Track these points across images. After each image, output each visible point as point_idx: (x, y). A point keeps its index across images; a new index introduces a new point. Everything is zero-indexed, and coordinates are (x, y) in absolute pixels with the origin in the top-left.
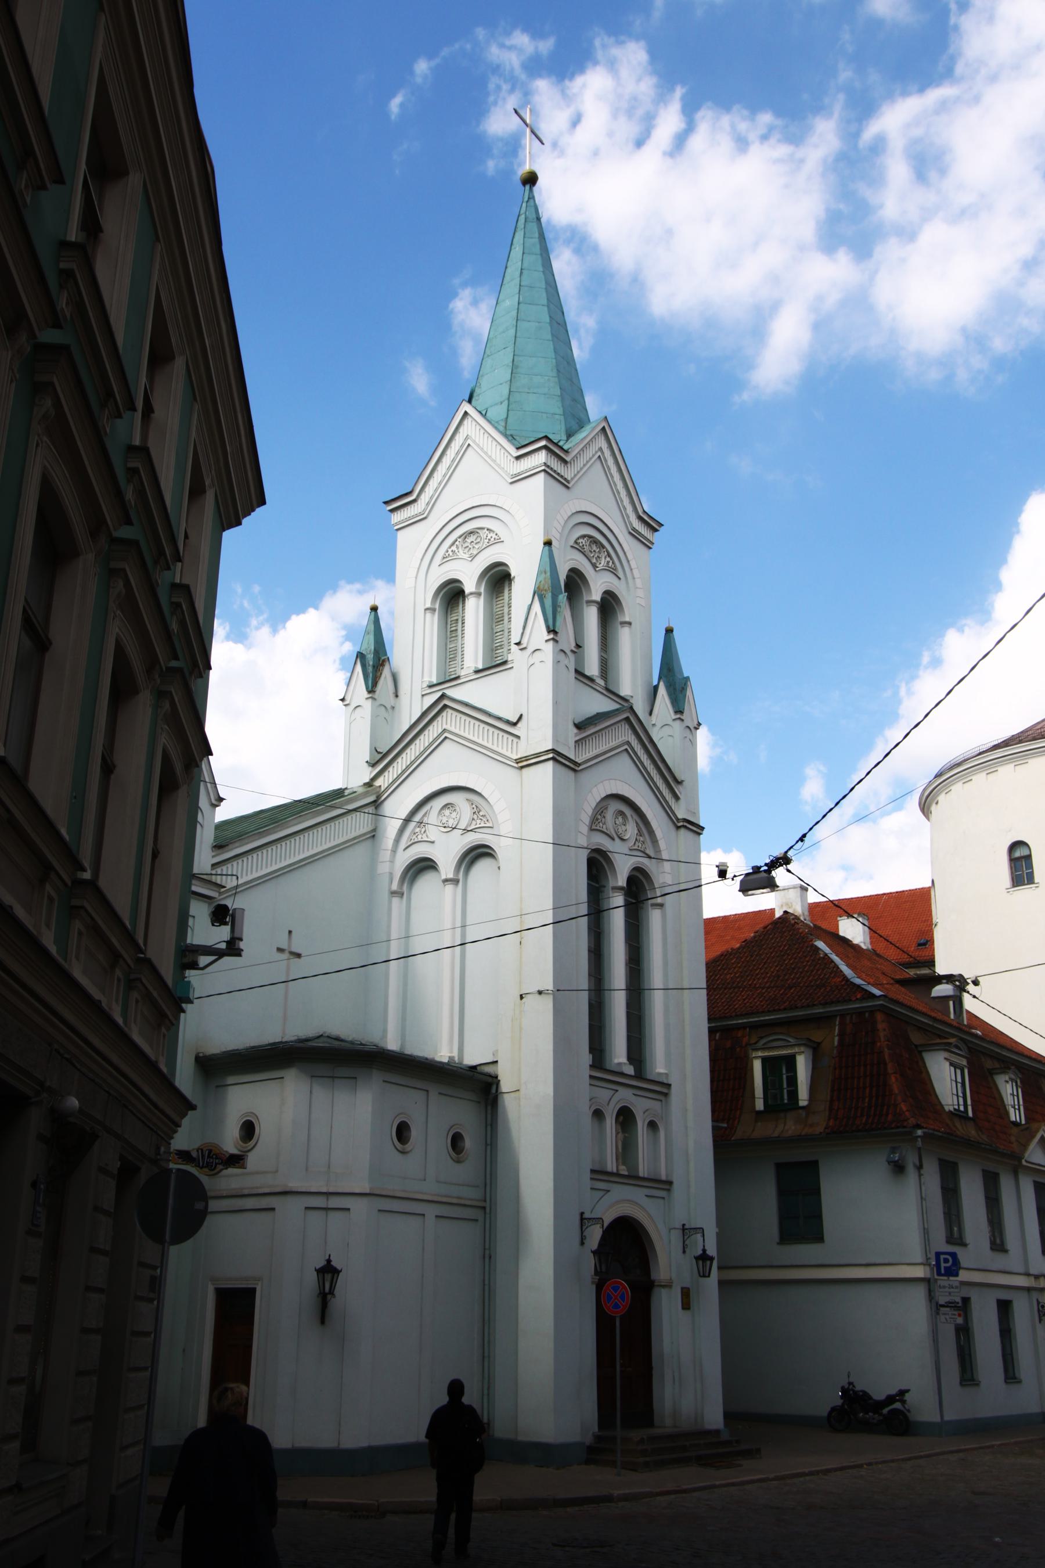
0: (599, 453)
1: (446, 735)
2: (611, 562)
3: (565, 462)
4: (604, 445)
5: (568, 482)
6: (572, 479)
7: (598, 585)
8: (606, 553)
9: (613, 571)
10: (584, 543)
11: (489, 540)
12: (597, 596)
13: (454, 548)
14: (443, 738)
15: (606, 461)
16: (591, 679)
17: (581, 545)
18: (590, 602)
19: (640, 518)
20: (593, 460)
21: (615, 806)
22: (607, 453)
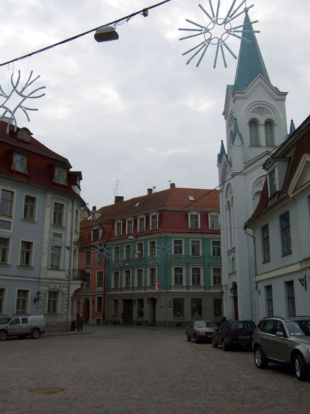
0: (260, 83)
2: (268, 111)
3: (244, 93)
6: (247, 96)
7: (262, 120)
8: (265, 109)
9: (270, 113)
15: (262, 84)
18: (260, 125)
19: (278, 95)
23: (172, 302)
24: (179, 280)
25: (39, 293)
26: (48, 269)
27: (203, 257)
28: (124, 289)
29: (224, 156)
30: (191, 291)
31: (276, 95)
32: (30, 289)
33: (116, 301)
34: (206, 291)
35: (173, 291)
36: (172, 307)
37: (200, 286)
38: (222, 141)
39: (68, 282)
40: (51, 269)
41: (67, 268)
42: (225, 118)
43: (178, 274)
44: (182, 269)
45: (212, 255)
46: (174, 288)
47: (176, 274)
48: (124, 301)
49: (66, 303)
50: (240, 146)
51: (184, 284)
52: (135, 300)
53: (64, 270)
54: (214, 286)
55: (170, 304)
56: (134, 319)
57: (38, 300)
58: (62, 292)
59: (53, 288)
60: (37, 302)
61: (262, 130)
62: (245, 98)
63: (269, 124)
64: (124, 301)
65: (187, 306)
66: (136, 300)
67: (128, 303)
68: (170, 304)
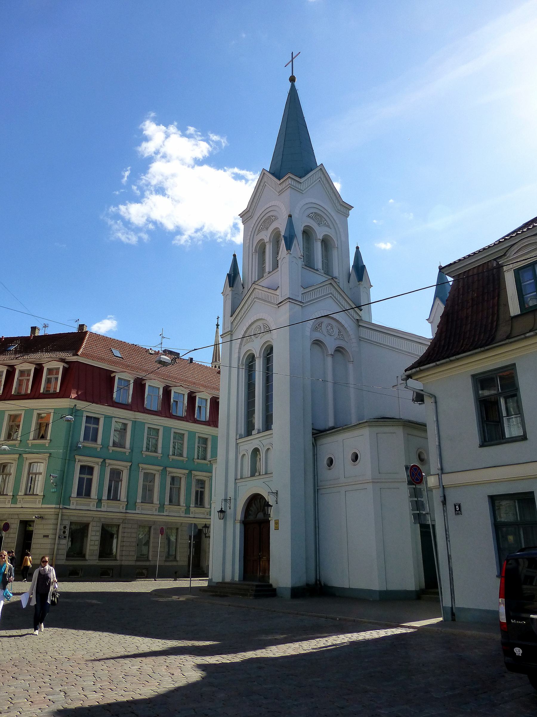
1: (255, 300)
3: (301, 183)
4: (322, 176)
5: (302, 191)
6: (305, 190)
7: (320, 232)
9: (328, 226)
10: (312, 216)
11: (272, 220)
12: (320, 236)
13: (261, 227)
14: (253, 302)
16: (317, 270)
17: (311, 217)
20: (317, 181)
21: (326, 321)
22: (324, 179)
23: (68, 528)
31: (338, 204)
34: (128, 511)
38: (235, 256)
43: (86, 477)
47: (83, 476)
50: (298, 259)
55: (64, 532)
61: (318, 248)
62: (300, 191)
63: (326, 242)
68: (64, 532)
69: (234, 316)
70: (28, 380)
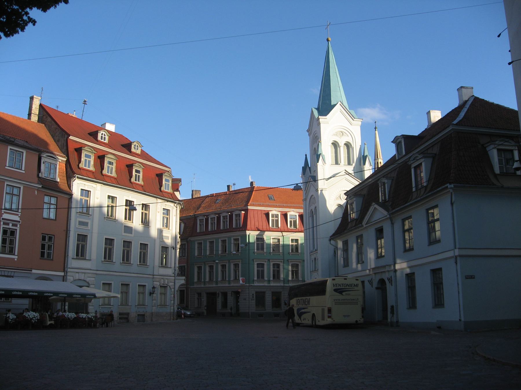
5: (328, 122)
23: (255, 295)
24: (261, 275)
25: (154, 288)
26: (159, 267)
27: (283, 253)
28: (208, 283)
29: (308, 169)
30: (272, 284)
32: (146, 284)
33: (200, 294)
34: (285, 285)
35: (255, 284)
36: (255, 300)
37: (280, 280)
38: (306, 155)
39: (173, 278)
40: (161, 267)
41: (173, 266)
42: (309, 135)
43: (260, 269)
44: (263, 264)
45: (291, 252)
46: (256, 282)
47: (258, 269)
48: (208, 294)
49: (172, 296)
51: (266, 279)
52: (219, 293)
53: (171, 268)
54: (292, 280)
55: (253, 297)
56: (218, 311)
57: (153, 293)
58: (170, 286)
59: (163, 283)
60: (151, 295)
64: (208, 294)
65: (269, 299)
66: (220, 293)
67: (212, 296)
68: (253, 297)
69: (306, 191)
70: (227, 221)
